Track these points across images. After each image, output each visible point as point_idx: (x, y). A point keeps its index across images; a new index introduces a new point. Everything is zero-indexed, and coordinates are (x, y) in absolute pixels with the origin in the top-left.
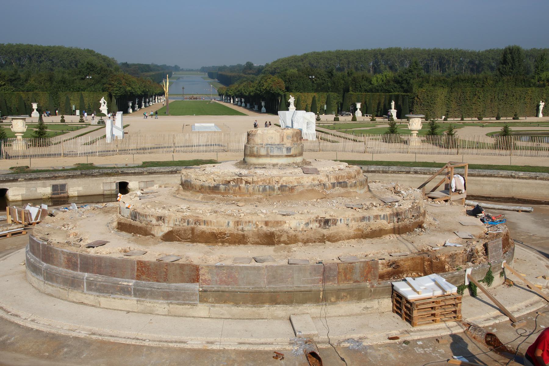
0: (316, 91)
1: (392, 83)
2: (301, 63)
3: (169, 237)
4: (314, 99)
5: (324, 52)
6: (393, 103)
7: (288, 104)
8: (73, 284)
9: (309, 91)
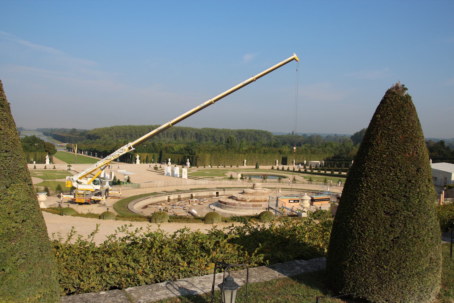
0: (148, 152)
1: (184, 150)
2: (110, 132)
3: (250, 201)
4: (147, 156)
5: (122, 126)
6: (188, 160)
7: (136, 159)
8: (241, 209)
9: (145, 153)
